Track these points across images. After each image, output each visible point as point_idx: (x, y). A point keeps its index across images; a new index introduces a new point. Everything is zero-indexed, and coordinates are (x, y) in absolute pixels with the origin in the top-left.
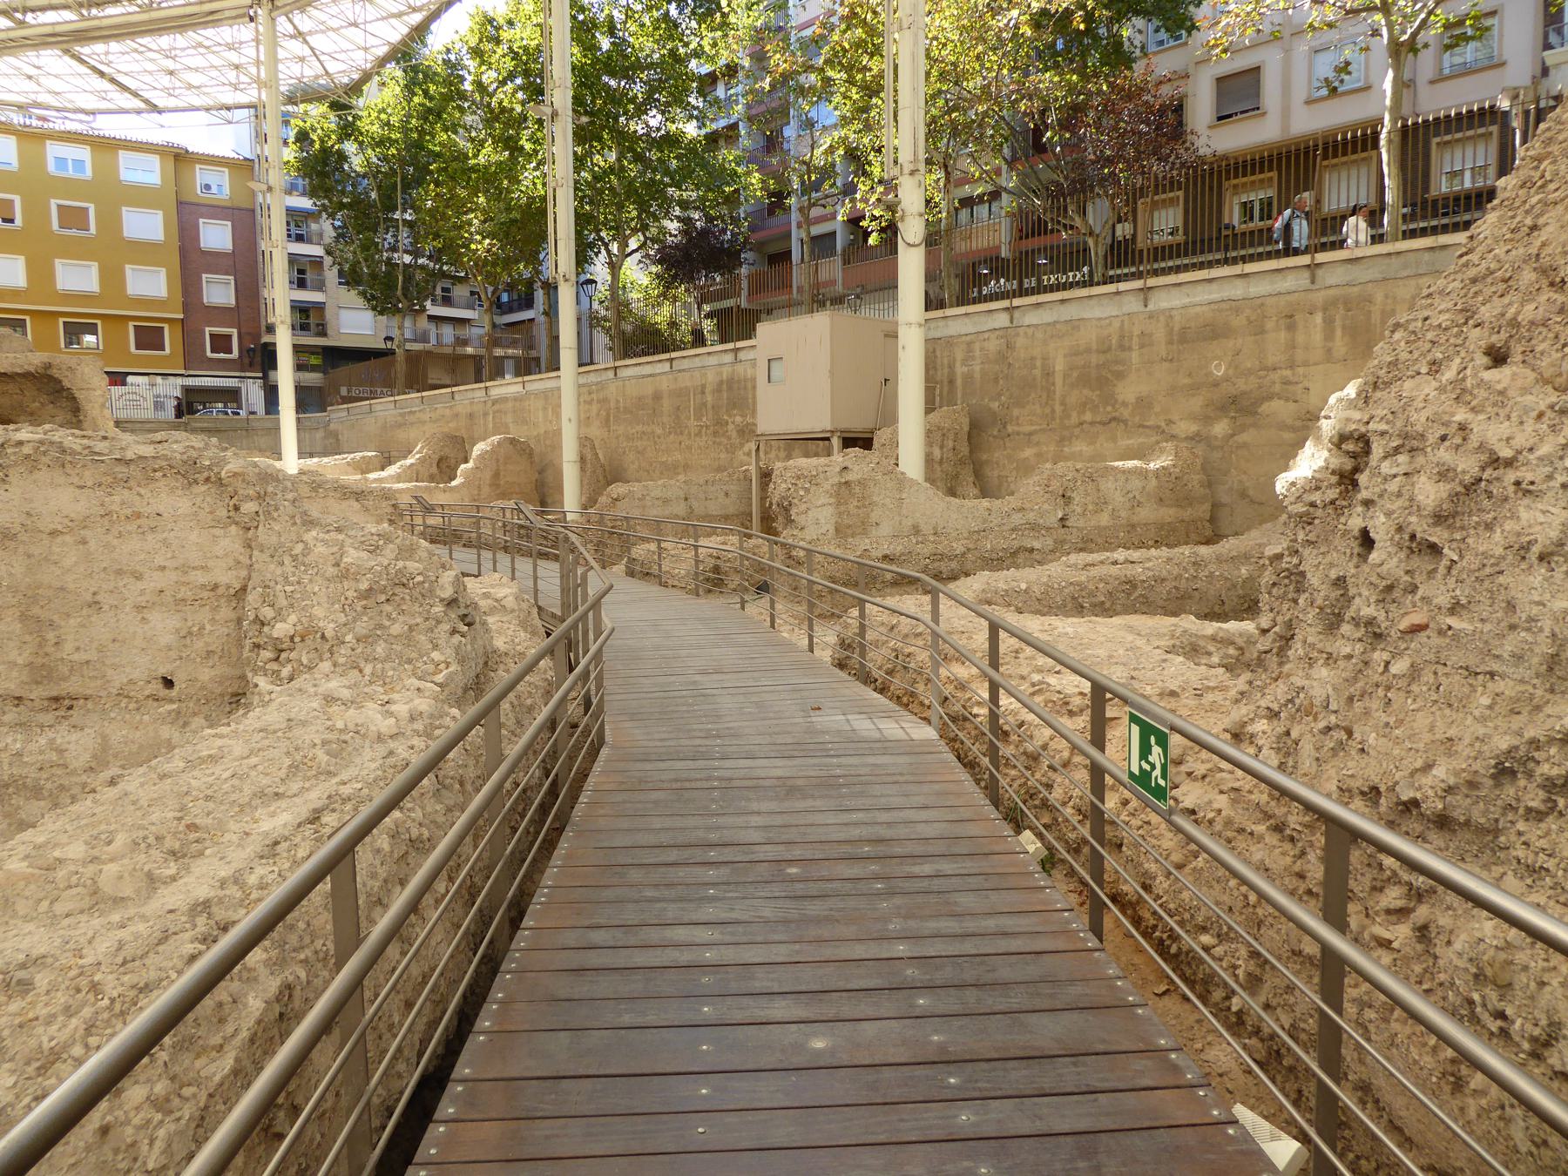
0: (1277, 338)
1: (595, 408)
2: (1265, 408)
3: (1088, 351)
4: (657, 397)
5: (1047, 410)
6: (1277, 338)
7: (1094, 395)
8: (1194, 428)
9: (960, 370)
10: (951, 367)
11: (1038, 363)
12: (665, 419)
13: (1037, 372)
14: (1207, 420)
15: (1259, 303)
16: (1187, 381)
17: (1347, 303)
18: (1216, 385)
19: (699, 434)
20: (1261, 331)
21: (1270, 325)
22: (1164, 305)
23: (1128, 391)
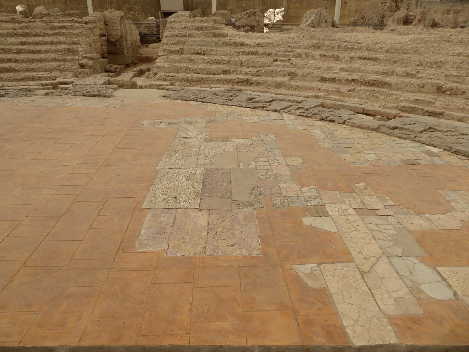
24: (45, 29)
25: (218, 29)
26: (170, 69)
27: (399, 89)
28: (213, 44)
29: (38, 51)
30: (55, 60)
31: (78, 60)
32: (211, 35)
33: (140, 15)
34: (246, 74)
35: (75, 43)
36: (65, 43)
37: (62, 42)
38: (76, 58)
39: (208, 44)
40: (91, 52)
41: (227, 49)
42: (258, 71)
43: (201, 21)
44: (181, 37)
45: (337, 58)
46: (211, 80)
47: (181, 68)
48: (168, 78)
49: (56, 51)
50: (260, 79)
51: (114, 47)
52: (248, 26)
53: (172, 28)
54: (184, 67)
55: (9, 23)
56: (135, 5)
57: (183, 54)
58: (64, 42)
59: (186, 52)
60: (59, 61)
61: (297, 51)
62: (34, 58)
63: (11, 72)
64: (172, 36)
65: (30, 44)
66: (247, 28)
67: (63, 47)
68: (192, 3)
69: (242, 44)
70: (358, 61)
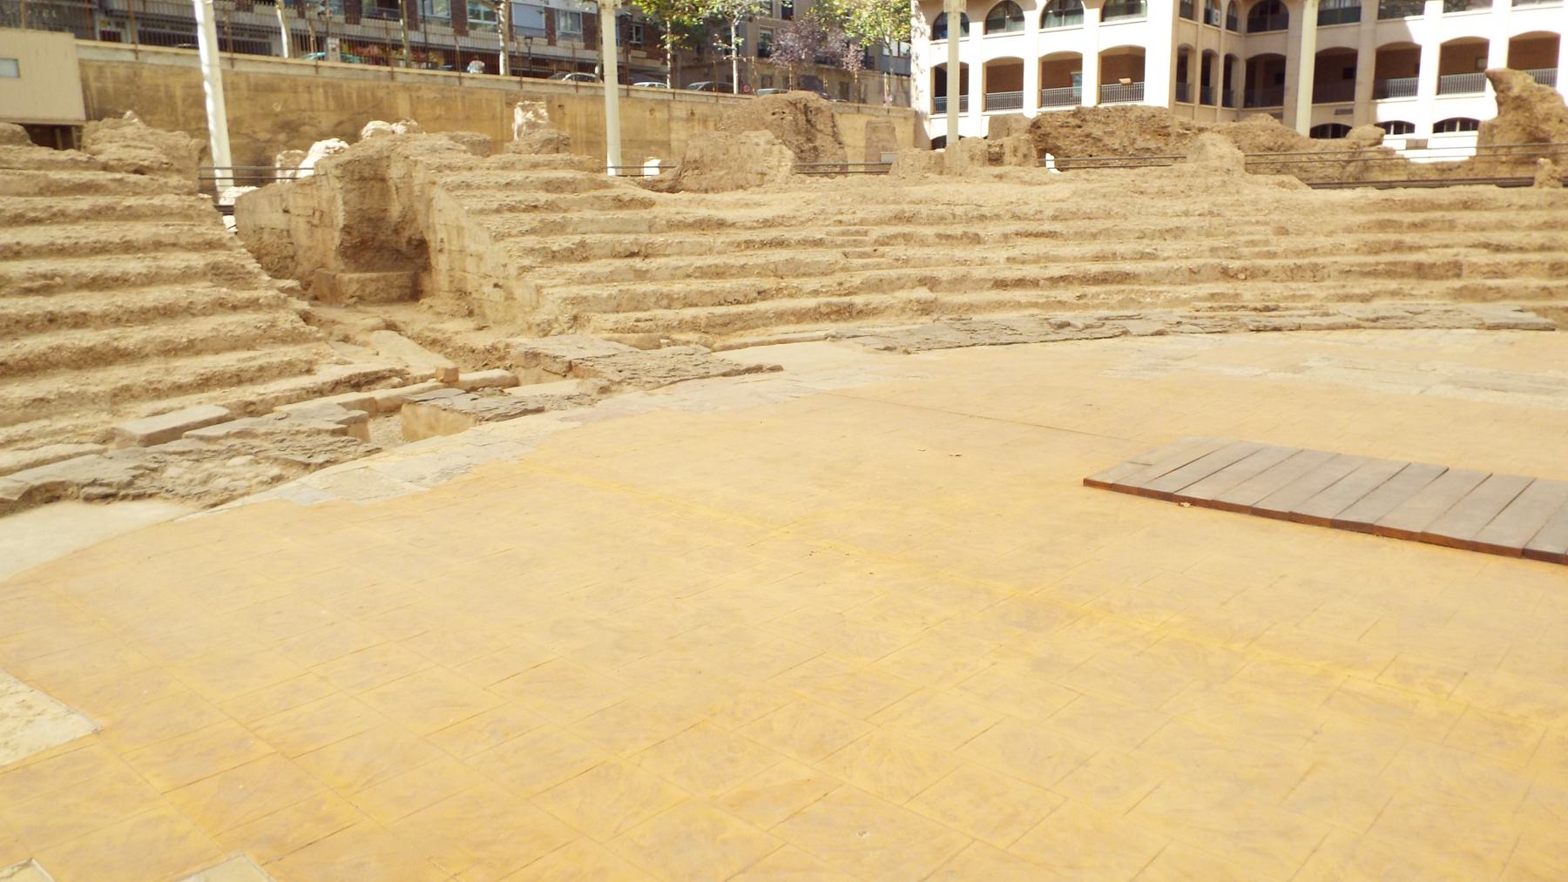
0: (304, 97)
6: (304, 97)
8: (268, 136)
13: (162, 94)
14: (275, 133)
15: (294, 79)
17: (333, 86)
18: (277, 115)
20: (295, 92)
24: (19, 194)
26: (614, 303)
27: (1156, 282)
29: (116, 279)
34: (816, 293)
36: (174, 245)
39: (631, 228)
41: (691, 237)
42: (840, 284)
43: (535, 166)
44: (524, 211)
45: (976, 239)
46: (760, 318)
47: (645, 294)
48: (641, 324)
49: (186, 276)
50: (876, 299)
53: (468, 186)
54: (654, 293)
57: (586, 259)
58: (172, 240)
60: (235, 308)
61: (876, 232)
62: (149, 304)
63: (110, 363)
64: (498, 211)
65: (38, 252)
69: (721, 224)
70: (1019, 241)
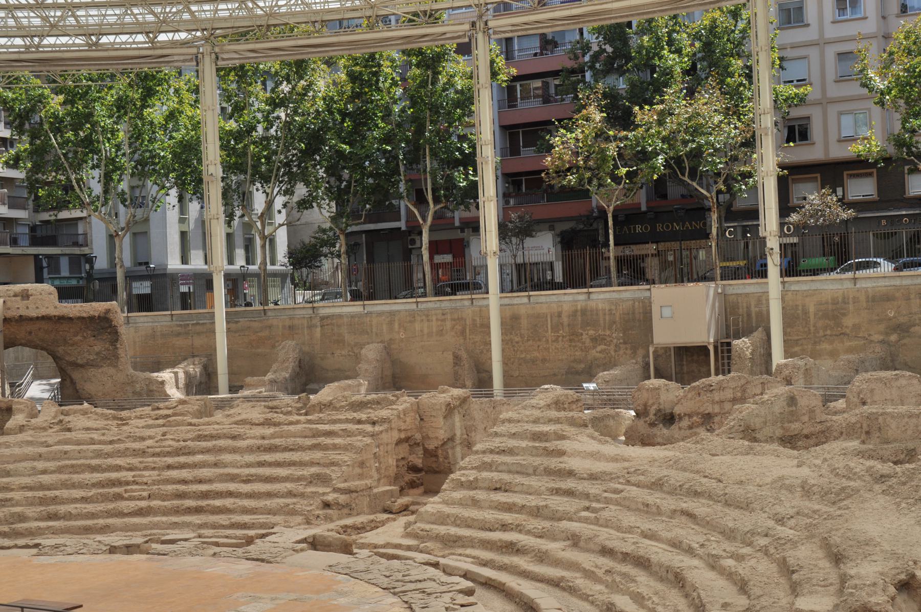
1: (449, 324)
2: (912, 330)
3: (827, 303)
4: (515, 318)
5: (806, 329)
7: (832, 323)
8: (881, 338)
9: (754, 310)
10: (748, 308)
11: (800, 308)
12: (523, 332)
14: (887, 334)
16: (877, 318)
18: (890, 319)
19: (556, 340)
21: (912, 296)
22: (864, 286)
23: (848, 321)
25: (562, 437)
28: (531, 471)
30: (290, 494)
31: (324, 494)
32: (542, 451)
33: (621, 352)
35: (333, 464)
37: (315, 461)
38: (321, 490)
40: (361, 476)
51: (434, 459)
52: (698, 414)
55: (260, 427)
56: (610, 328)
59: (480, 484)
60: (295, 496)
66: (695, 418)
67: (314, 470)
68: (749, 315)
69: (571, 473)
